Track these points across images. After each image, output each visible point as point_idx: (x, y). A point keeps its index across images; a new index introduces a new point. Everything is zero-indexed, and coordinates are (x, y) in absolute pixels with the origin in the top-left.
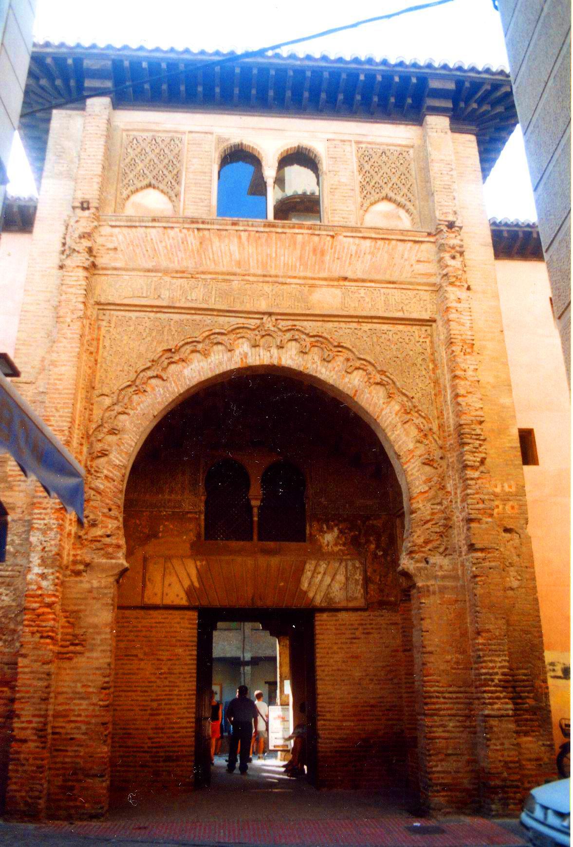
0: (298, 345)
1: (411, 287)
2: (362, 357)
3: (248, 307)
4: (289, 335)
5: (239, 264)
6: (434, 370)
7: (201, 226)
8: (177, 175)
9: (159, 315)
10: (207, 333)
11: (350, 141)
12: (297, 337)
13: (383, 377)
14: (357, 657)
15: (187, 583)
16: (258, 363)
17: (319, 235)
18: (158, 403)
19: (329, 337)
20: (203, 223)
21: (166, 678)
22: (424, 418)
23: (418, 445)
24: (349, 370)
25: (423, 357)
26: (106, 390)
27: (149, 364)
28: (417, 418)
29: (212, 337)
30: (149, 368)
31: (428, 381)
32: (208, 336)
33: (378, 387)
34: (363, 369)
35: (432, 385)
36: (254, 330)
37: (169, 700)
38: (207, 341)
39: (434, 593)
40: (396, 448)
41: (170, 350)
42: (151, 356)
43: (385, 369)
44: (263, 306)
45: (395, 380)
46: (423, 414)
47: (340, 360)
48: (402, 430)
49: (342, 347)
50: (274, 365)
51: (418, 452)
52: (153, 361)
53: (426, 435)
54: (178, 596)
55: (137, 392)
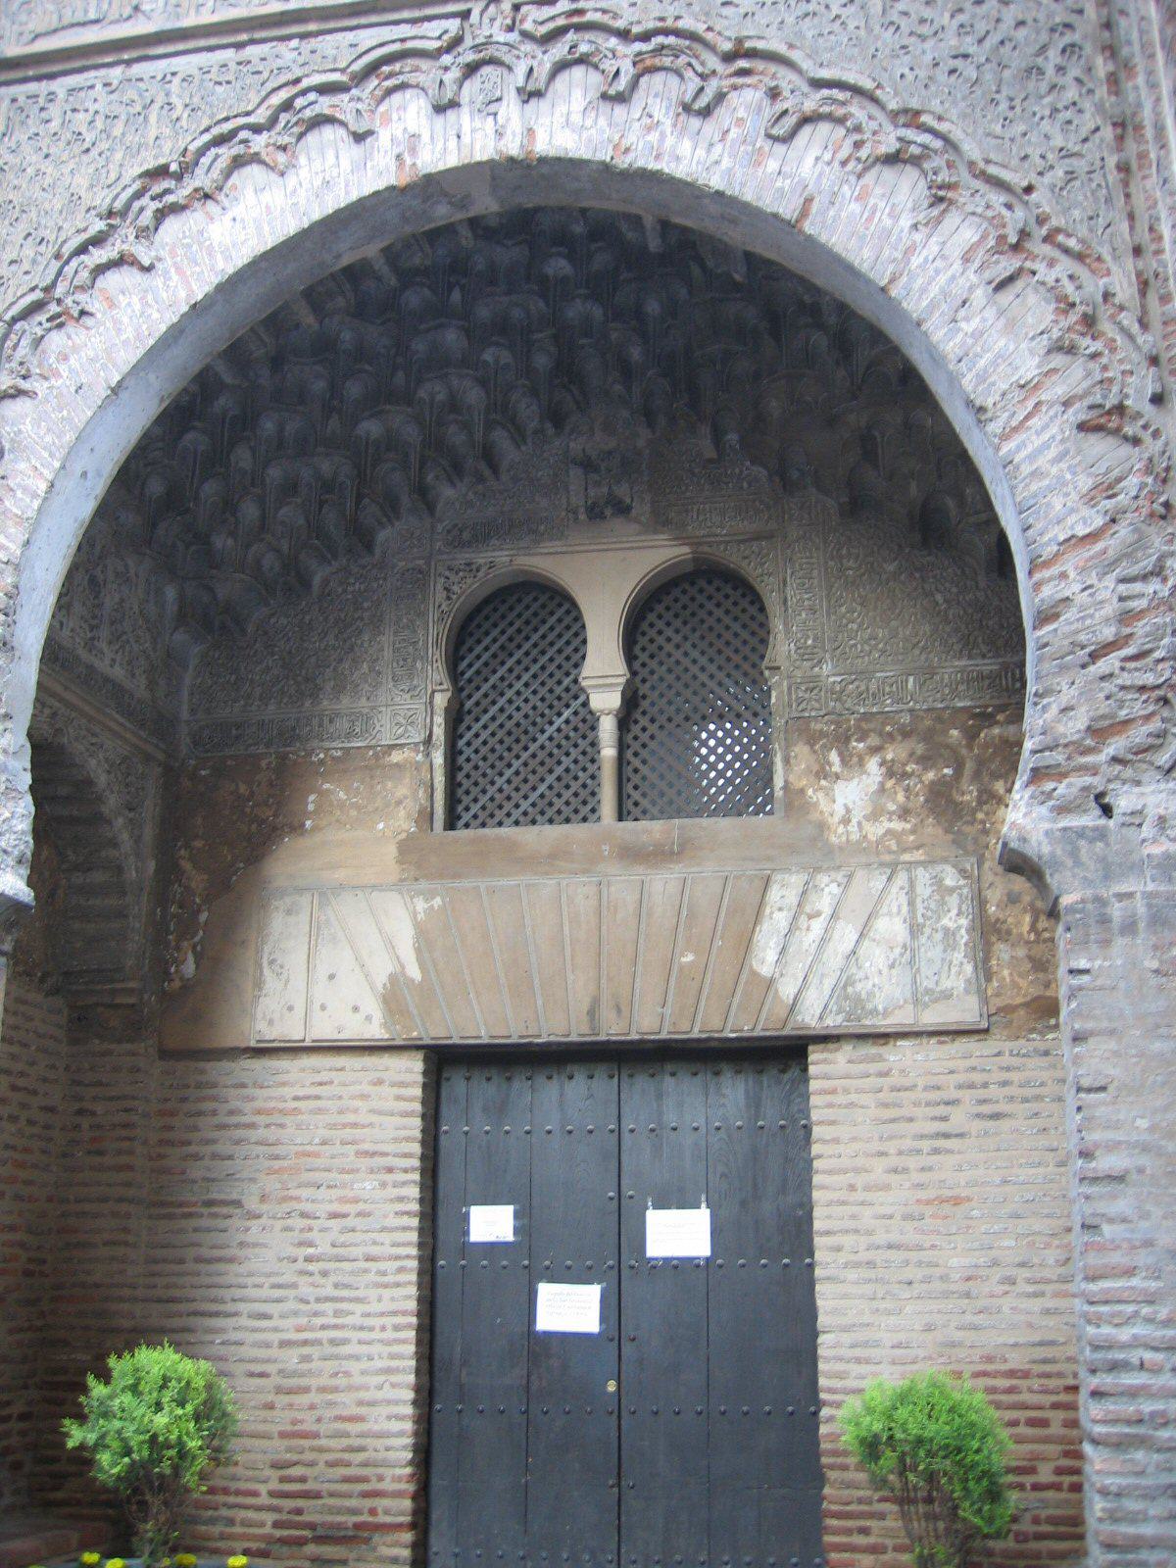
0: (595, 78)
2: (825, 74)
4: (559, 50)
6: (1113, 81)
9: (138, 69)
12: (584, 48)
13: (910, 134)
14: (957, 1201)
15: (382, 970)
16: (452, 161)
18: (126, 343)
19: (700, 28)
21: (324, 1274)
22: (1080, 257)
23: (1058, 360)
25: (1068, 38)
28: (1052, 263)
29: (299, 103)
30: (98, 241)
31: (1088, 120)
32: (287, 106)
33: (888, 174)
34: (829, 117)
35: (1108, 133)
37: (333, 1342)
38: (284, 117)
39: (1129, 927)
40: (968, 382)
41: (162, 172)
42: (102, 199)
43: (914, 104)
45: (957, 134)
46: (1072, 243)
47: (746, 104)
48: (990, 313)
49: (752, 54)
50: (512, 160)
51: (1057, 390)
52: (110, 214)
53: (1089, 322)
54: (356, 1009)
55: (58, 322)
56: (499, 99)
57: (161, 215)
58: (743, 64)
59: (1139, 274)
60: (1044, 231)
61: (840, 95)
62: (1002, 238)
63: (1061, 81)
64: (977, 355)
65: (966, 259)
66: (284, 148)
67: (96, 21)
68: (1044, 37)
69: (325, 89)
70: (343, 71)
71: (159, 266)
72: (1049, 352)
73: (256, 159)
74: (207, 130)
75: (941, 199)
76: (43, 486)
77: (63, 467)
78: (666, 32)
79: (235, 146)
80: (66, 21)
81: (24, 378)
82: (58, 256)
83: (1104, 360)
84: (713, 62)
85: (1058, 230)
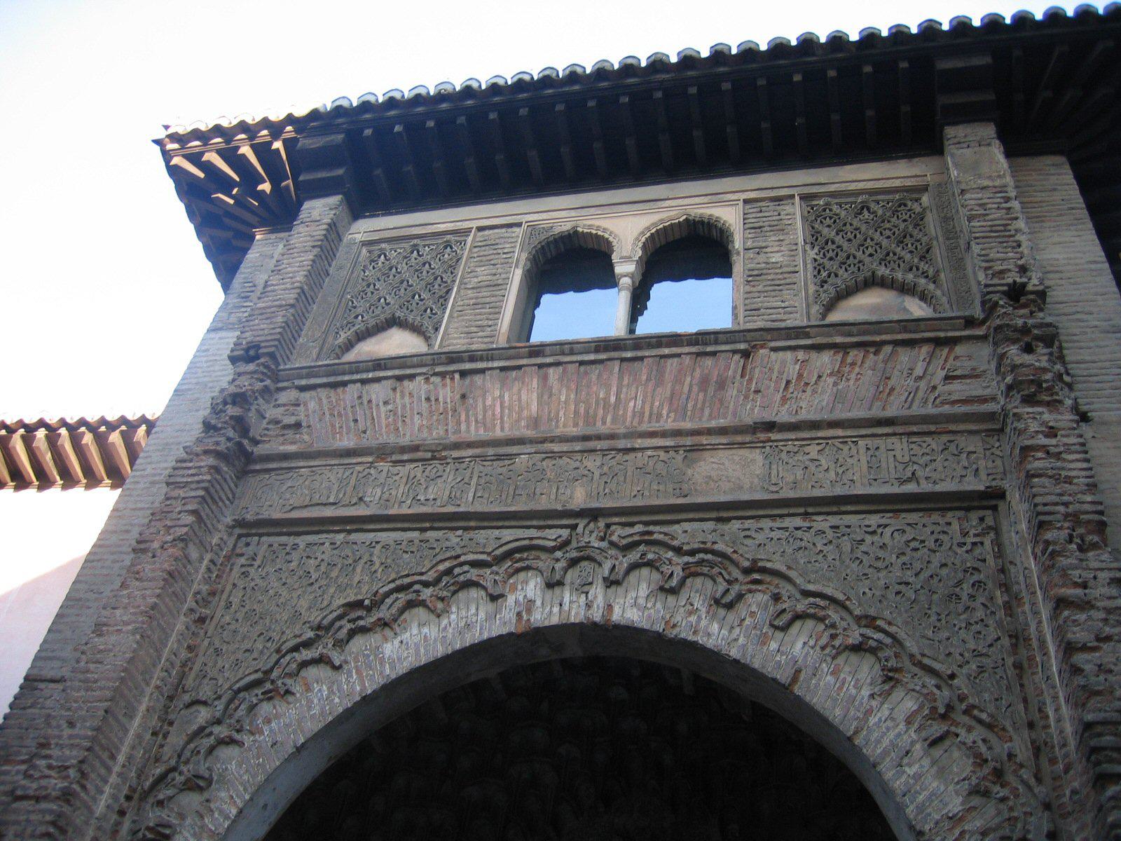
0: (656, 576)
1: (933, 428)
2: (811, 587)
3: (544, 504)
4: (634, 556)
5: (535, 422)
6: (1008, 607)
7: (468, 366)
8: (444, 298)
9: (354, 536)
10: (447, 564)
11: (792, 197)
12: (650, 556)
13: (869, 632)
16: (555, 620)
17: (714, 354)
18: (312, 717)
19: (729, 551)
20: (472, 359)
22: (990, 727)
23: (976, 801)
24: (779, 623)
25: (976, 577)
26: (206, 692)
27: (311, 634)
28: (970, 729)
30: (307, 644)
31: (992, 633)
32: (449, 572)
33: (854, 658)
34: (813, 616)
35: (1006, 641)
36: (553, 549)
38: (445, 580)
40: (910, 811)
41: (358, 604)
42: (315, 617)
43: (872, 612)
44: (579, 497)
45: (902, 635)
46: (984, 716)
47: (757, 601)
48: (926, 762)
49: (763, 570)
50: (595, 624)
51: (977, 823)
52: (319, 627)
53: (998, 774)
55: (269, 696)
56: (591, 583)
57: (352, 634)
58: (756, 576)
59: (1033, 742)
60: (963, 707)
61: (822, 603)
62: (934, 709)
63: (972, 604)
64: (917, 792)
65: (909, 722)
66: (442, 599)
67: (334, 504)
68: (960, 575)
69: (475, 564)
70: (489, 554)
71: (345, 667)
72: (970, 794)
73: (422, 604)
74: (393, 581)
75: (891, 679)
76: (234, 811)
77: (251, 799)
78: (706, 551)
79: (411, 596)
80: (314, 501)
81: (238, 731)
82: (278, 651)
83: (1011, 803)
84: (736, 573)
85: (974, 707)
